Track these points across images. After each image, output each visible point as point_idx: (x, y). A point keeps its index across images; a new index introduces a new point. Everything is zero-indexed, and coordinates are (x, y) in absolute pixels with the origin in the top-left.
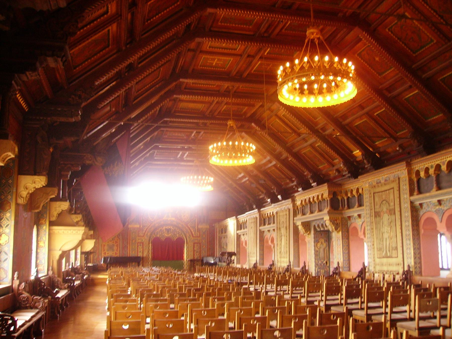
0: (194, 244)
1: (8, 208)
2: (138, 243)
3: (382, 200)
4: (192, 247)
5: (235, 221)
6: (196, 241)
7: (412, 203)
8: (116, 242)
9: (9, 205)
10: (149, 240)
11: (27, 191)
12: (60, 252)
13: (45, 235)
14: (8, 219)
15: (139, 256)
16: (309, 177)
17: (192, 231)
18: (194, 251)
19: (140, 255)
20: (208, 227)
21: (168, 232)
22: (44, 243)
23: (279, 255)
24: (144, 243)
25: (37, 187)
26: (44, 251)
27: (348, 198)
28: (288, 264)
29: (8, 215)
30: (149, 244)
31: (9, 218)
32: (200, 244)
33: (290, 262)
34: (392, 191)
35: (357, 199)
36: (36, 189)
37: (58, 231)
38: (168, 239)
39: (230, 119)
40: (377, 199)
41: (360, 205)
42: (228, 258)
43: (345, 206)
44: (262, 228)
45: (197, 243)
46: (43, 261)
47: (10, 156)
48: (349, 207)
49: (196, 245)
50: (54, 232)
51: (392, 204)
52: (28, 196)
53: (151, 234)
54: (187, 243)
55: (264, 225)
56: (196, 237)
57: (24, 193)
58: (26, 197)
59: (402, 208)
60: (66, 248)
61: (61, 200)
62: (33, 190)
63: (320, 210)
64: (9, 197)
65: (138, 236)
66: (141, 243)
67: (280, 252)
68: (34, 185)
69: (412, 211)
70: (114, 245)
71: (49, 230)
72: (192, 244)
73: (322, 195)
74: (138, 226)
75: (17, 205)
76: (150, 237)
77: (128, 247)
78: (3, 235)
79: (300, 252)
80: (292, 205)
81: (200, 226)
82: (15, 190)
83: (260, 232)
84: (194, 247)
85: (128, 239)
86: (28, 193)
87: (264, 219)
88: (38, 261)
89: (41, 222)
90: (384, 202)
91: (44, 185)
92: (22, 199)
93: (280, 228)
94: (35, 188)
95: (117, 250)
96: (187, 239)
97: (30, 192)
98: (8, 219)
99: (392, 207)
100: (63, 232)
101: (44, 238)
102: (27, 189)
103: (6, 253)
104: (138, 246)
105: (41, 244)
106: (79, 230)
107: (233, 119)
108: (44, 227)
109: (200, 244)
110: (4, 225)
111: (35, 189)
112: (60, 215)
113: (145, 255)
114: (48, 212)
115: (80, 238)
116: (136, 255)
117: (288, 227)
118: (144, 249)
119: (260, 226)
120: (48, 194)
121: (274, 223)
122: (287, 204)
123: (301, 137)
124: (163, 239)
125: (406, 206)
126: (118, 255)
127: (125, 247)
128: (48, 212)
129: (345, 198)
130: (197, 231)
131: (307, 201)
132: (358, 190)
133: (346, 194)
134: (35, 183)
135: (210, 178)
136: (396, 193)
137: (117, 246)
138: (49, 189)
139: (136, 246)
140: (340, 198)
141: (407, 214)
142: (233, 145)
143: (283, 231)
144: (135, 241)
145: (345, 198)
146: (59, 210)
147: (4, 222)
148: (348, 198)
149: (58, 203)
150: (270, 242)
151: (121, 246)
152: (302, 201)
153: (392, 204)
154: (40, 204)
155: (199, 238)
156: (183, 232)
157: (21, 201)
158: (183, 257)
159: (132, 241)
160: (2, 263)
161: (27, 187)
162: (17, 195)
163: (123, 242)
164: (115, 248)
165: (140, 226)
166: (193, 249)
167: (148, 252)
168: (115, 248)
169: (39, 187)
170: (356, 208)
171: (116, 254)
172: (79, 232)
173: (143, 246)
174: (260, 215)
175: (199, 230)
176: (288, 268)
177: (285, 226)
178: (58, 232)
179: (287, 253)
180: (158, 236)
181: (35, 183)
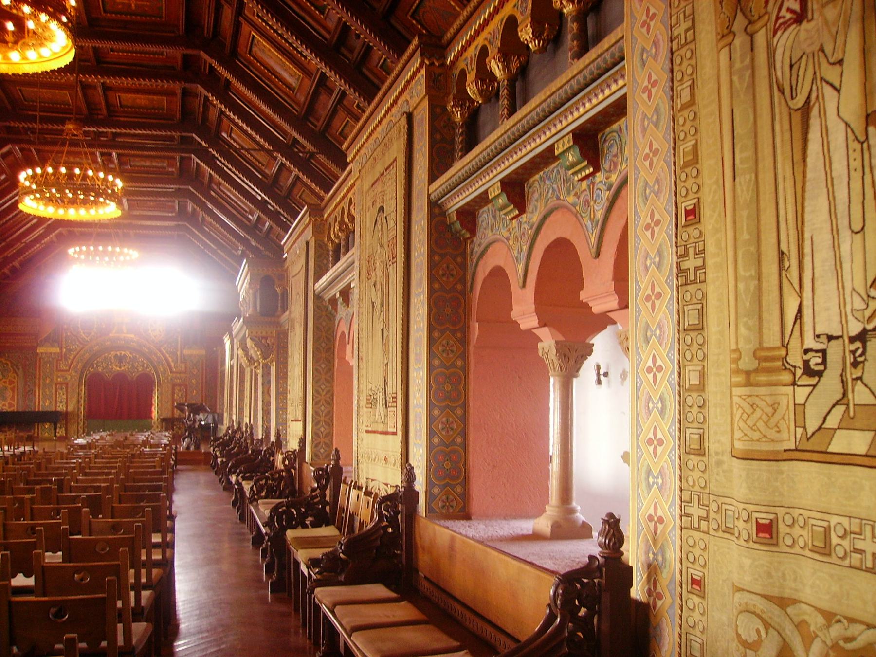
0: (174, 386)
4: (170, 392)
8: (11, 382)
15: (59, 409)
17: (170, 360)
19: (61, 408)
21: (120, 361)
30: (80, 385)
32: (186, 386)
38: (121, 376)
39: (69, 119)
42: (189, 415)
45: (180, 385)
49: (177, 389)
53: (84, 367)
54: (159, 384)
56: (177, 373)
66: (61, 384)
72: (170, 386)
74: (58, 350)
76: (82, 373)
81: (186, 352)
84: (173, 393)
85: (35, 377)
95: (13, 398)
104: (56, 391)
107: (76, 120)
109: (186, 386)
113: (70, 409)
116: (54, 410)
124: (109, 376)
126: (15, 409)
127: (29, 393)
130: (181, 362)
135: (131, 251)
137: (13, 389)
139: (54, 391)
142: (70, 176)
144: (52, 380)
155: (183, 375)
156: (152, 362)
158: (151, 412)
163: (26, 382)
164: (9, 394)
166: (170, 397)
167: (78, 401)
168: (9, 394)
171: (11, 405)
173: (67, 388)
175: (184, 359)
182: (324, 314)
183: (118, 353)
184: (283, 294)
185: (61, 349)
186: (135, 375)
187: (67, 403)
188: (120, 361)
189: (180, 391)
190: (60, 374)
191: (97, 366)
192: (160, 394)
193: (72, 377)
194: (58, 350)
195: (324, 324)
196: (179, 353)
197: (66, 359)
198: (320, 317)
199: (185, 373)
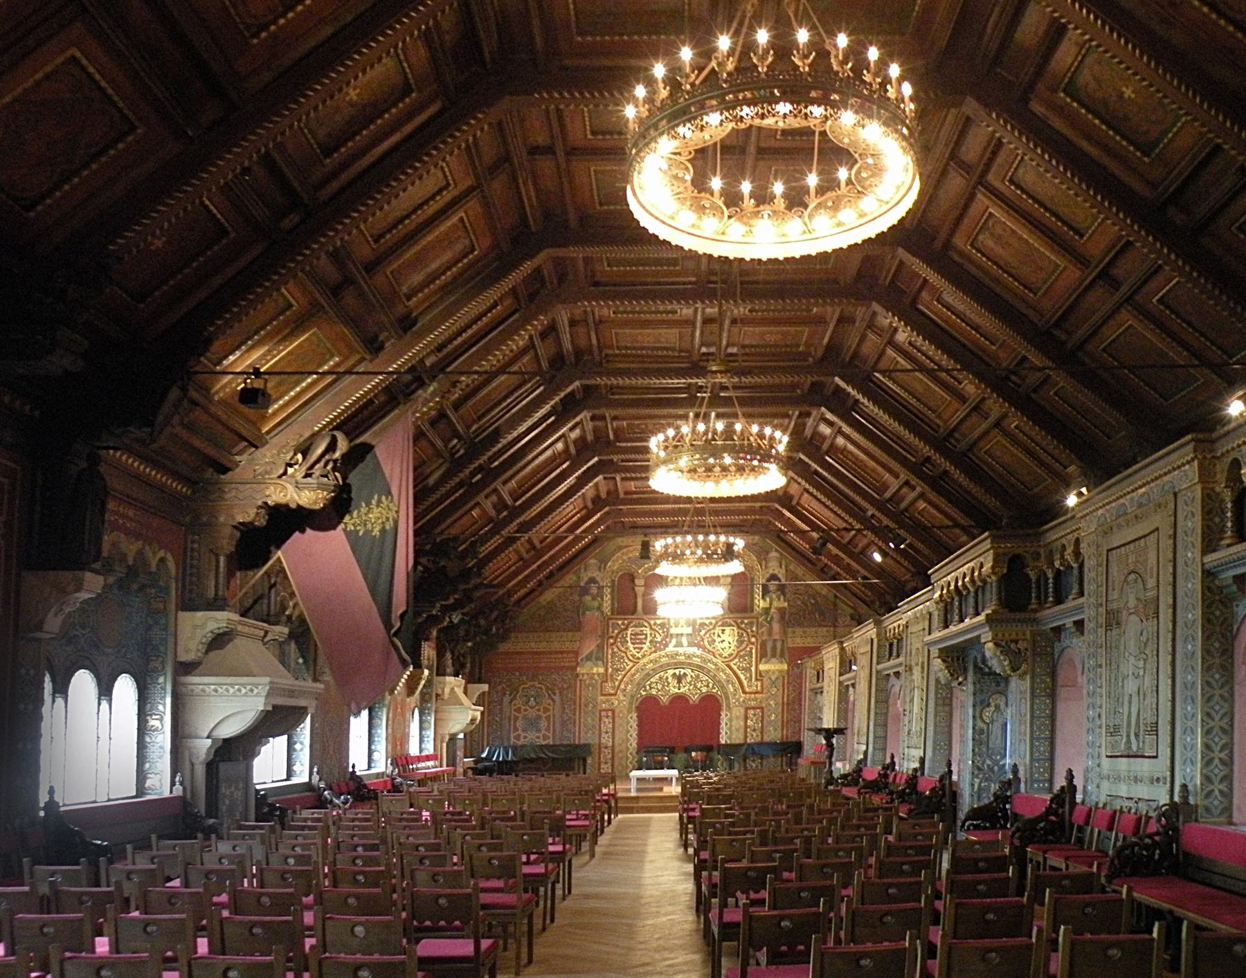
3: (1126, 571)
5: (837, 651)
7: (1208, 574)
10: (631, 704)
13: (164, 697)
17: (742, 677)
20: (785, 667)
21: (679, 682)
27: (1058, 574)
34: (1153, 538)
35: (1076, 572)
40: (1114, 570)
41: (1081, 594)
43: (1047, 597)
48: (1059, 600)
51: (1151, 583)
59: (1180, 593)
63: (978, 614)
69: (1207, 605)
70: (539, 717)
73: (982, 566)
74: (601, 670)
76: (632, 697)
81: (762, 667)
87: (891, 645)
90: (1133, 576)
99: (1151, 594)
106: (256, 686)
125: (1192, 586)
129: (1050, 575)
131: (952, 587)
132: (1077, 540)
133: (1051, 564)
136: (1166, 543)
137: (548, 718)
140: (1033, 575)
141: (1193, 614)
145: (1050, 575)
148: (1058, 574)
151: (558, 721)
153: (1151, 583)
159: (586, 706)
165: (606, 670)
170: (1070, 604)
174: (878, 635)
175: (760, 676)
180: (654, 692)
182: (1217, 598)
184: (1038, 581)
188: (679, 682)
190: (603, 698)
193: (621, 702)
194: (601, 670)
195: (1218, 613)
196: (753, 669)
197: (612, 681)
198: (1213, 602)
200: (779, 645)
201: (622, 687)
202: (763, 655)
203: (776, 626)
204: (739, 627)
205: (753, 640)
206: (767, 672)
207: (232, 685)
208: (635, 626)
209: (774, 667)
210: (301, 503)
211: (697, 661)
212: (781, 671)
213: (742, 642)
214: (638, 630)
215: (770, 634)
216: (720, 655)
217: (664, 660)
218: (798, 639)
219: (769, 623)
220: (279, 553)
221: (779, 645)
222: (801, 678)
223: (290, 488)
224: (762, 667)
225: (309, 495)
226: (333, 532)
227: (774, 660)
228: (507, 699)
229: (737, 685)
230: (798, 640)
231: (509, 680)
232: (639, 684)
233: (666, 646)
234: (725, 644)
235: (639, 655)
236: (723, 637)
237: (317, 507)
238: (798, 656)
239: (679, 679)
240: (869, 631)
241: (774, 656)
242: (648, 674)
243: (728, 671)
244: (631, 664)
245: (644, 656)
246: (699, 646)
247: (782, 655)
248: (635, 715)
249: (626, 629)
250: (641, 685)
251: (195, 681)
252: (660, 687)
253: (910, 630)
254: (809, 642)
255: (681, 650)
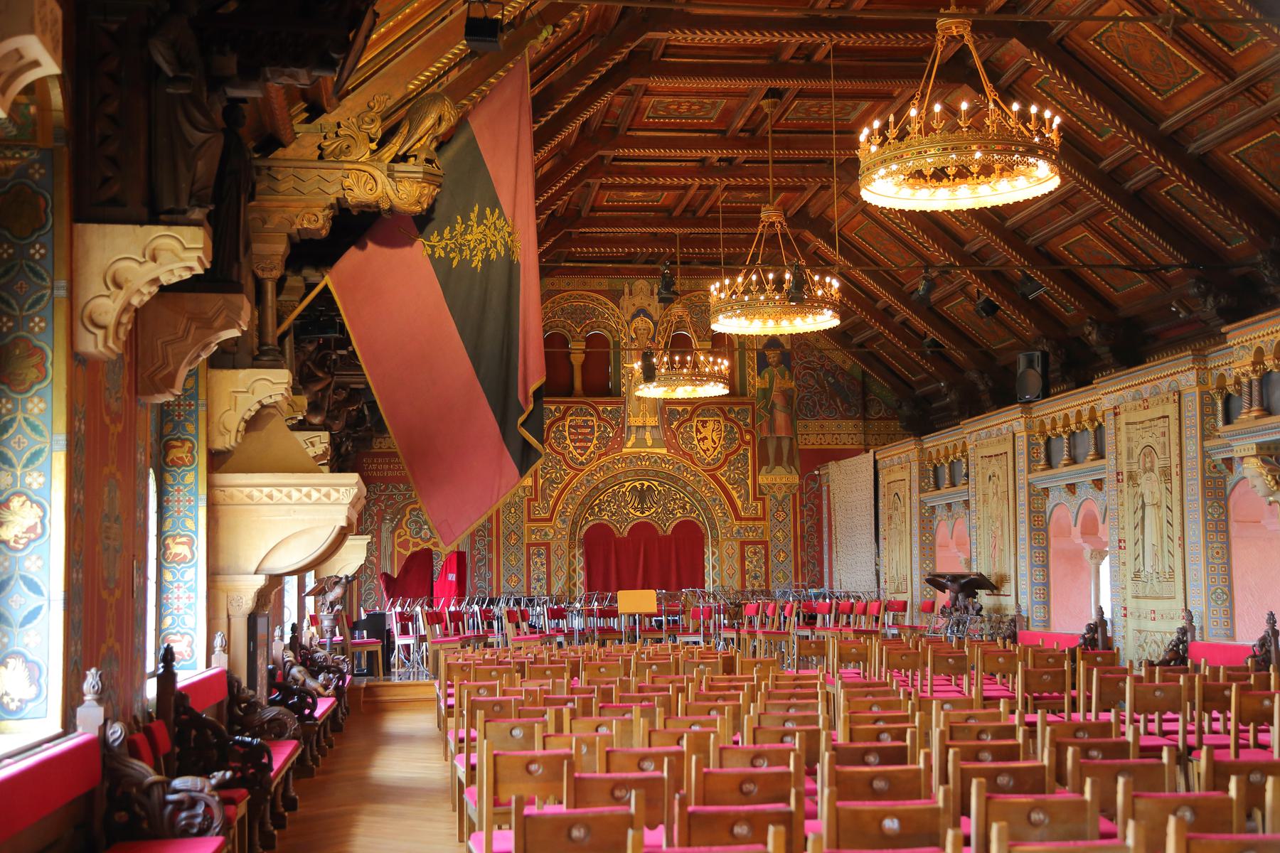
1: (33, 374)
2: (529, 545)
4: (737, 555)
5: (914, 455)
6: (751, 536)
9: (36, 359)
10: (573, 534)
11: (121, 296)
12: (260, 581)
14: (34, 428)
16: (1260, 257)
18: (744, 572)
20: (795, 479)
21: (642, 501)
22: (190, 544)
23: (1129, 584)
24: (553, 547)
25: (166, 280)
26: (190, 574)
28: (1181, 623)
29: (35, 406)
31: (44, 420)
32: (765, 543)
33: (1189, 616)
36: (164, 289)
37: (247, 490)
44: (1042, 478)
46: (190, 621)
47: (36, 64)
49: (749, 549)
50: (231, 497)
52: (125, 319)
55: (1050, 464)
57: (108, 307)
58: (119, 324)
60: (281, 563)
61: (257, 361)
62: (149, 291)
64: (38, 324)
65: (530, 520)
67: (1137, 575)
68: (151, 270)
71: (211, 486)
72: (736, 546)
75: (77, 359)
76: (574, 523)
77: (491, 560)
78: (16, 503)
79: (1236, 574)
80: (1192, 376)
81: (763, 479)
82: (61, 293)
83: (1030, 495)
84: (743, 558)
85: (490, 535)
86: (127, 307)
87: (1048, 441)
88: (168, 621)
89: (175, 454)
91: (200, 271)
92: (100, 333)
93: (1131, 477)
94: (155, 281)
96: (713, 527)
97: (136, 301)
98: (34, 428)
100: (270, 497)
101: (190, 524)
102: (119, 286)
103: (33, 587)
105: (176, 549)
108: (190, 478)
110: (19, 454)
111: (155, 289)
112: (253, 423)
114: (202, 414)
115: (339, 517)
117: (1174, 470)
118: (553, 567)
119: (1030, 472)
120: (209, 326)
121: (1100, 455)
122: (1177, 375)
123: (1238, 81)
128: (202, 414)
130: (755, 499)
134: (154, 259)
138: (213, 302)
139: (524, 558)
143: (1150, 486)
144: (520, 538)
146: (248, 406)
147: (20, 441)
149: (244, 376)
150: (1076, 531)
152: (1260, 352)
154: (176, 371)
156: (700, 501)
157: (92, 344)
159: (508, 538)
160: (16, 630)
161: (121, 279)
162: (76, 316)
165: (536, 482)
166: (737, 566)
167: (570, 578)
169: (175, 280)
172: (334, 495)
174: (1028, 428)
175: (759, 494)
176: (1180, 641)
177: (1158, 464)
178: (250, 497)
179: (1172, 575)
181: (154, 259)
183: (637, 484)
185: (536, 482)
186: (669, 528)
187: (767, 580)
189: (755, 553)
190: (534, 525)
191: (601, 510)
192: (720, 560)
193: (557, 532)
196: (749, 482)
199: (764, 519)
200: (785, 445)
201: (560, 507)
202: (762, 460)
203: (780, 417)
204: (727, 419)
205: (748, 437)
206: (770, 486)
207: (298, 486)
208: (576, 414)
209: (781, 478)
210: (396, 201)
211: (668, 468)
212: (790, 487)
213: (733, 440)
214: (580, 420)
215: (772, 429)
216: (702, 460)
217: (620, 467)
218: (814, 435)
219: (771, 411)
220: (328, 280)
221: (785, 445)
222: (820, 497)
223: (381, 177)
224: (763, 479)
225: (404, 191)
226: (407, 250)
227: (778, 468)
228: (387, 526)
229: (727, 506)
230: (812, 439)
231: (390, 497)
232: (582, 503)
233: (622, 444)
234: (709, 444)
235: (583, 459)
236: (705, 432)
237: (418, 209)
238: (813, 462)
239: (642, 495)
240: (1010, 421)
241: (778, 462)
242: (596, 488)
243: (713, 485)
244: (572, 473)
245: (589, 461)
246: (669, 446)
247: (791, 462)
248: (578, 552)
249: (563, 418)
250: (587, 505)
251: (238, 484)
252: (613, 508)
253: (1123, 418)
254: (828, 443)
255: (644, 451)
